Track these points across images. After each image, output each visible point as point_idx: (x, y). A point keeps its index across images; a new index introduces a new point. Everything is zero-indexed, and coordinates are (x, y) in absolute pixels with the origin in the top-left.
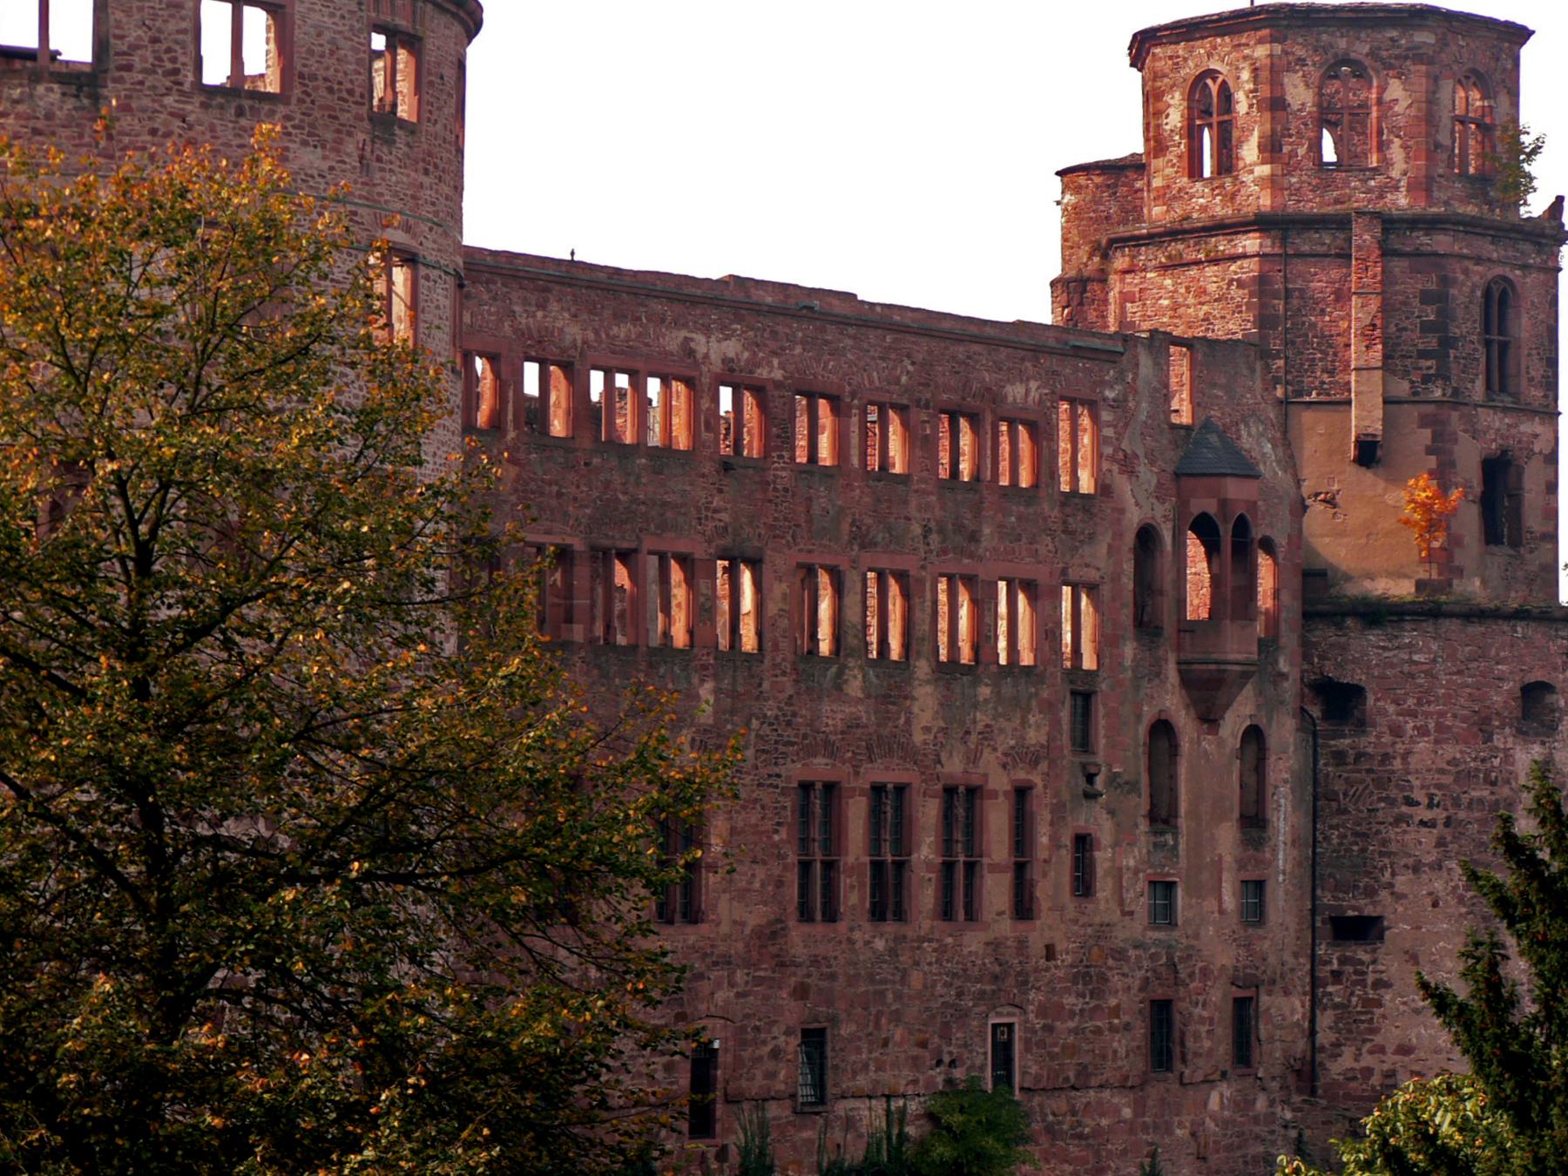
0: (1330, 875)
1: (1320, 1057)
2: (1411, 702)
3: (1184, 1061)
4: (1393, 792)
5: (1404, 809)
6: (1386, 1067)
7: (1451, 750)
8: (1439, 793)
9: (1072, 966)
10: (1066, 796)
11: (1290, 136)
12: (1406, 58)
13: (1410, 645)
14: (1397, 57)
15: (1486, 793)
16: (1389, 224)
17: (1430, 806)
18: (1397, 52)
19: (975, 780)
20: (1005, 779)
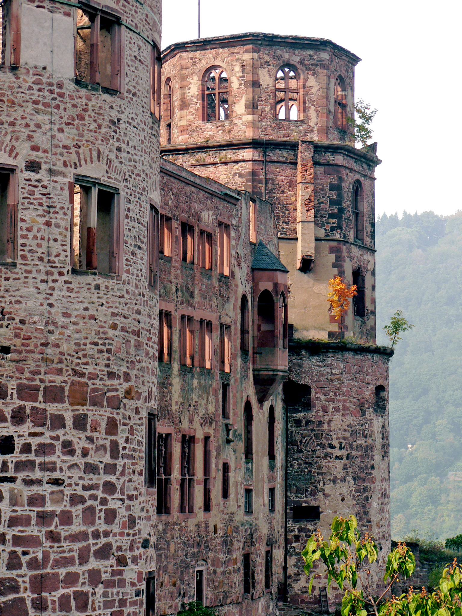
0: (294, 485)
1: (289, 581)
2: (332, 394)
3: (254, 587)
4: (324, 441)
5: (329, 450)
6: (321, 585)
7: (349, 420)
8: (344, 442)
9: (222, 537)
10: (220, 442)
11: (262, 101)
12: (317, 65)
13: (331, 365)
14: (312, 65)
15: (363, 442)
16: (317, 148)
17: (341, 448)
18: (313, 62)
19: (192, 433)
20: (202, 433)
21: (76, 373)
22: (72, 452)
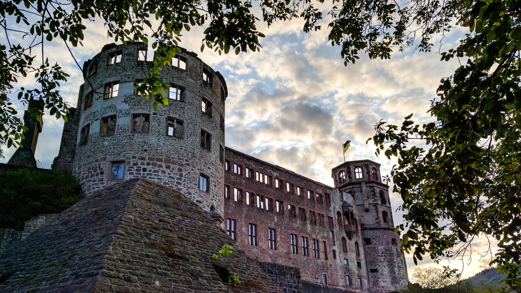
21: (166, 156)
22: (165, 173)
